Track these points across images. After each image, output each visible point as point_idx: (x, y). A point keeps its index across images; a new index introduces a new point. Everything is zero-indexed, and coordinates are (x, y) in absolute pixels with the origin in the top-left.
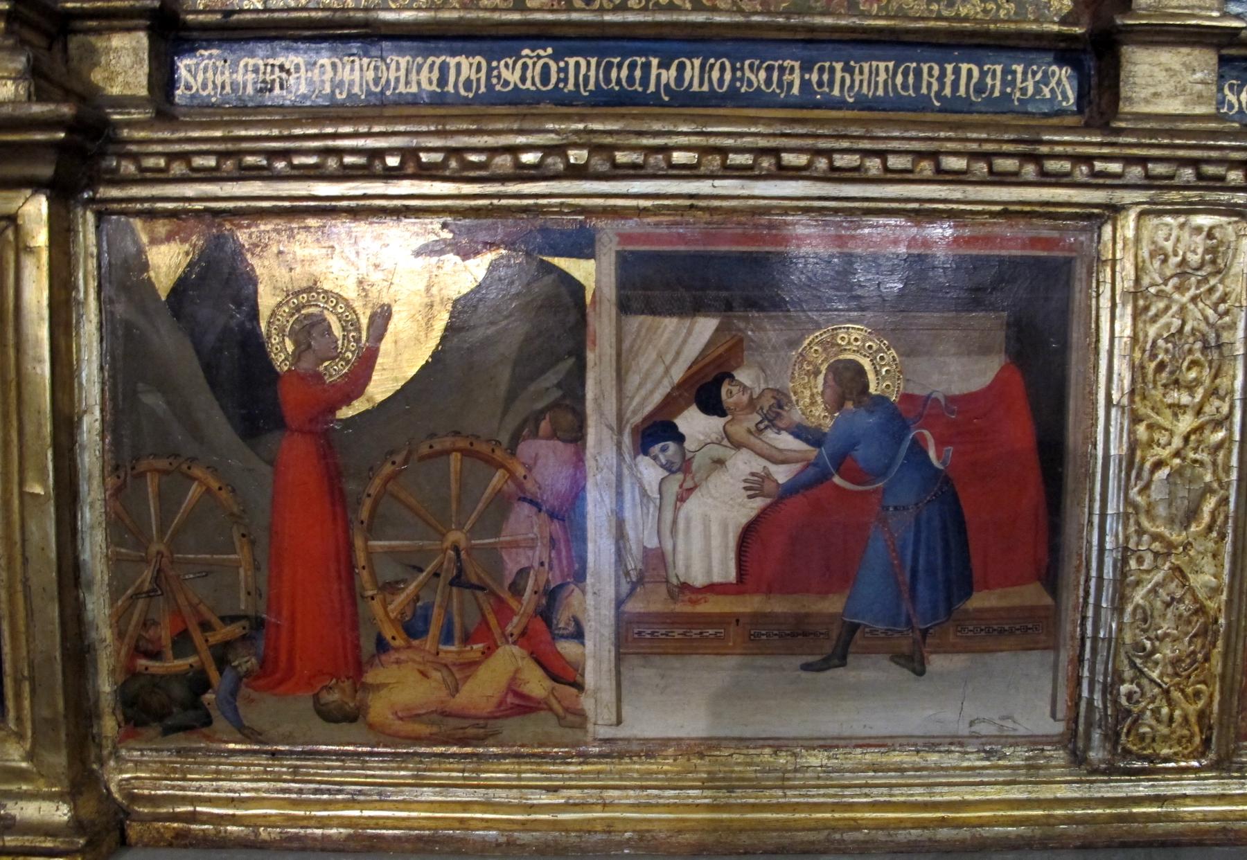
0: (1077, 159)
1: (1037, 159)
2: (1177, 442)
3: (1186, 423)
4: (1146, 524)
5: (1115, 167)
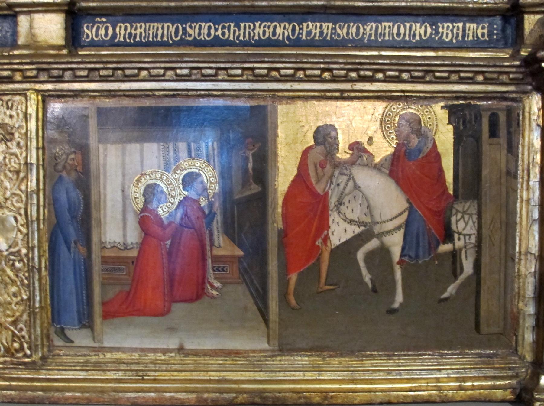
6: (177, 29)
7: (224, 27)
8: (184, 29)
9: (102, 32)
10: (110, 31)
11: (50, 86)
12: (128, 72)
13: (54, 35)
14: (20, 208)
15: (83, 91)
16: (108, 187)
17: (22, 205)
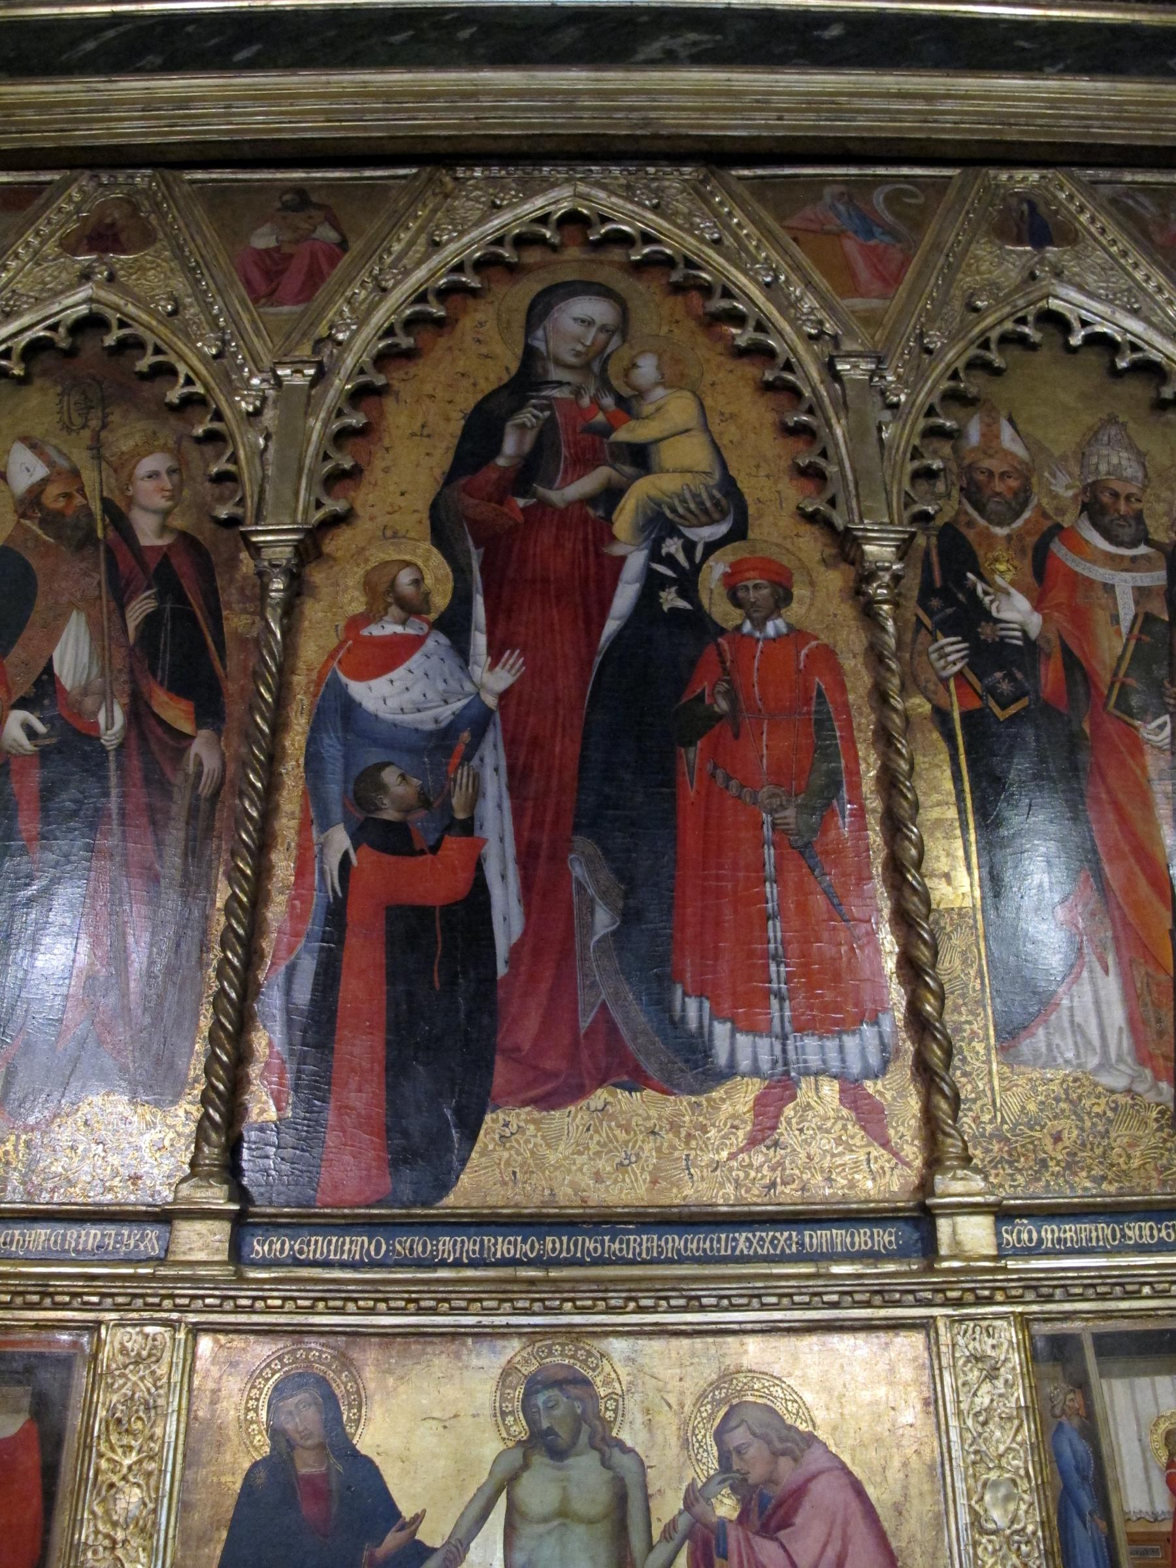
0: (74, 1295)
1: (51, 1295)
2: (125, 1470)
3: (134, 1457)
4: (101, 1527)
5: (95, 1299)
6: (1114, 1230)
7: (1167, 1227)
8: (1122, 1230)
9: (1025, 1236)
10: (1035, 1236)
11: (1035, 1308)
12: (1129, 1288)
13: (984, 1243)
14: (1018, 1468)
15: (1075, 1312)
16: (1121, 1435)
17: (1021, 1464)
